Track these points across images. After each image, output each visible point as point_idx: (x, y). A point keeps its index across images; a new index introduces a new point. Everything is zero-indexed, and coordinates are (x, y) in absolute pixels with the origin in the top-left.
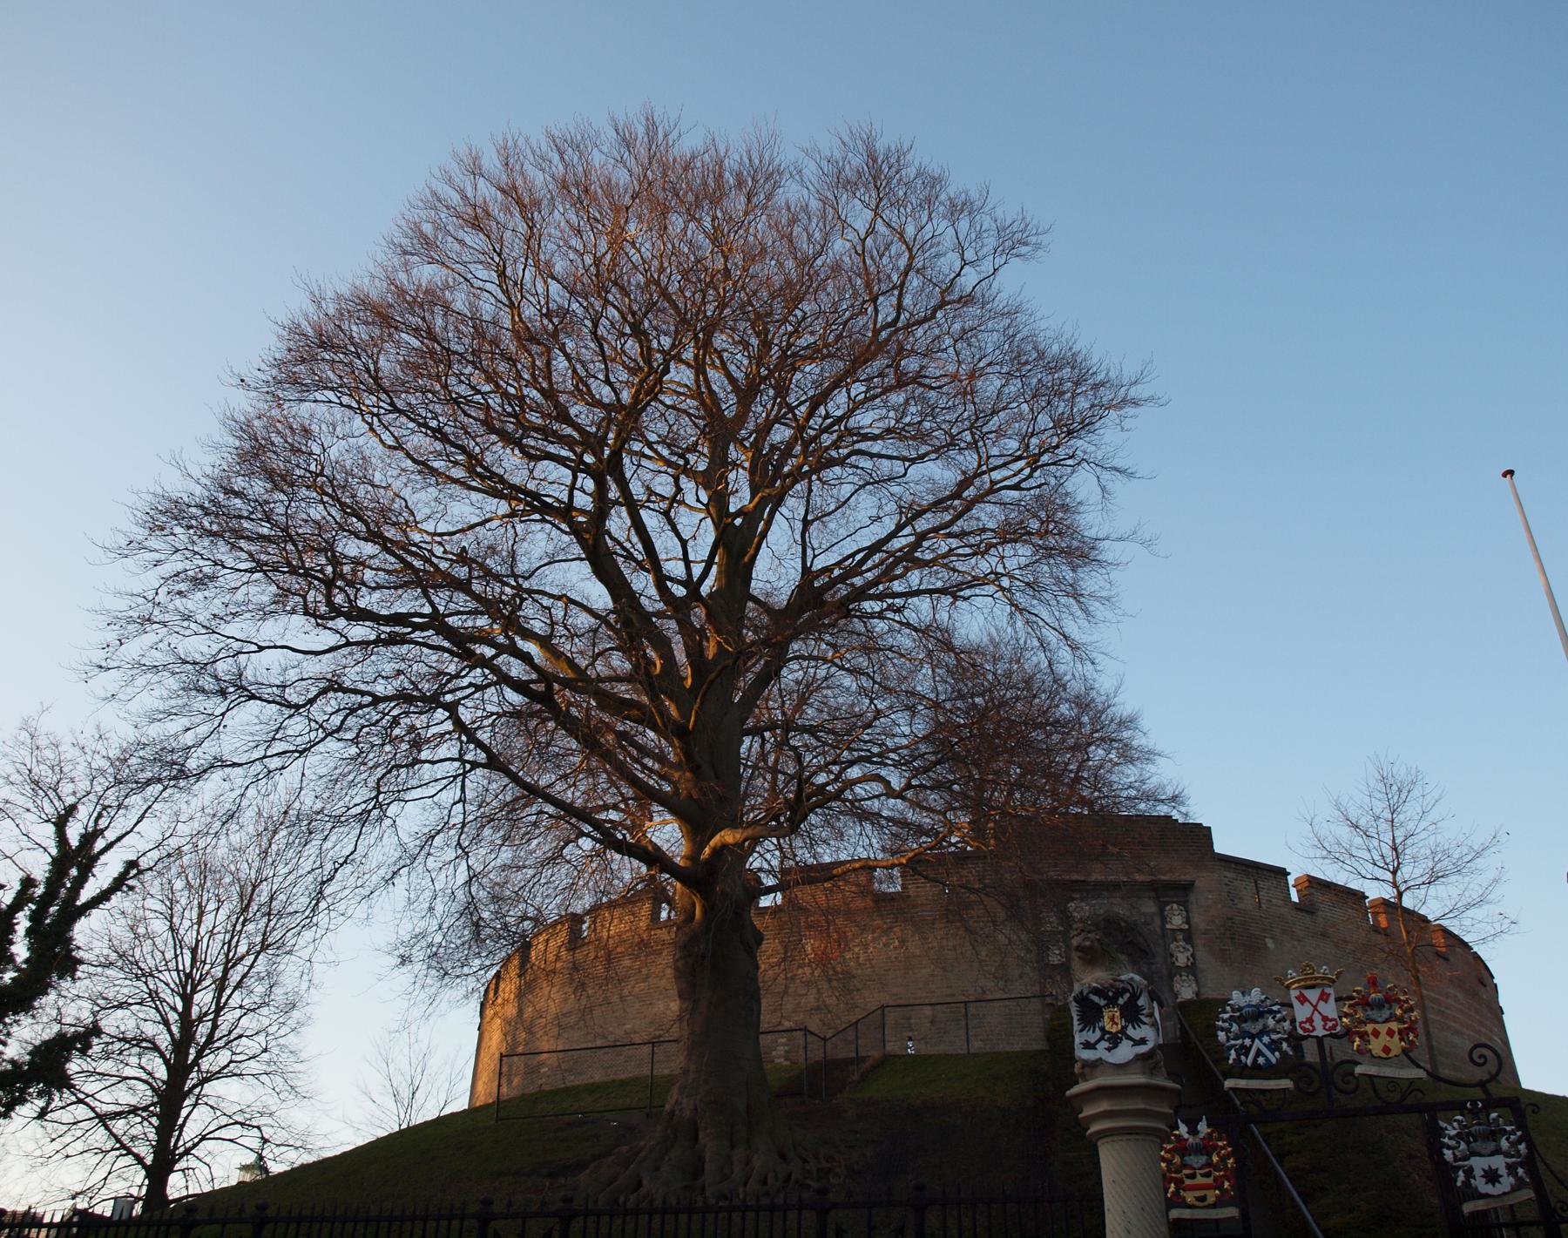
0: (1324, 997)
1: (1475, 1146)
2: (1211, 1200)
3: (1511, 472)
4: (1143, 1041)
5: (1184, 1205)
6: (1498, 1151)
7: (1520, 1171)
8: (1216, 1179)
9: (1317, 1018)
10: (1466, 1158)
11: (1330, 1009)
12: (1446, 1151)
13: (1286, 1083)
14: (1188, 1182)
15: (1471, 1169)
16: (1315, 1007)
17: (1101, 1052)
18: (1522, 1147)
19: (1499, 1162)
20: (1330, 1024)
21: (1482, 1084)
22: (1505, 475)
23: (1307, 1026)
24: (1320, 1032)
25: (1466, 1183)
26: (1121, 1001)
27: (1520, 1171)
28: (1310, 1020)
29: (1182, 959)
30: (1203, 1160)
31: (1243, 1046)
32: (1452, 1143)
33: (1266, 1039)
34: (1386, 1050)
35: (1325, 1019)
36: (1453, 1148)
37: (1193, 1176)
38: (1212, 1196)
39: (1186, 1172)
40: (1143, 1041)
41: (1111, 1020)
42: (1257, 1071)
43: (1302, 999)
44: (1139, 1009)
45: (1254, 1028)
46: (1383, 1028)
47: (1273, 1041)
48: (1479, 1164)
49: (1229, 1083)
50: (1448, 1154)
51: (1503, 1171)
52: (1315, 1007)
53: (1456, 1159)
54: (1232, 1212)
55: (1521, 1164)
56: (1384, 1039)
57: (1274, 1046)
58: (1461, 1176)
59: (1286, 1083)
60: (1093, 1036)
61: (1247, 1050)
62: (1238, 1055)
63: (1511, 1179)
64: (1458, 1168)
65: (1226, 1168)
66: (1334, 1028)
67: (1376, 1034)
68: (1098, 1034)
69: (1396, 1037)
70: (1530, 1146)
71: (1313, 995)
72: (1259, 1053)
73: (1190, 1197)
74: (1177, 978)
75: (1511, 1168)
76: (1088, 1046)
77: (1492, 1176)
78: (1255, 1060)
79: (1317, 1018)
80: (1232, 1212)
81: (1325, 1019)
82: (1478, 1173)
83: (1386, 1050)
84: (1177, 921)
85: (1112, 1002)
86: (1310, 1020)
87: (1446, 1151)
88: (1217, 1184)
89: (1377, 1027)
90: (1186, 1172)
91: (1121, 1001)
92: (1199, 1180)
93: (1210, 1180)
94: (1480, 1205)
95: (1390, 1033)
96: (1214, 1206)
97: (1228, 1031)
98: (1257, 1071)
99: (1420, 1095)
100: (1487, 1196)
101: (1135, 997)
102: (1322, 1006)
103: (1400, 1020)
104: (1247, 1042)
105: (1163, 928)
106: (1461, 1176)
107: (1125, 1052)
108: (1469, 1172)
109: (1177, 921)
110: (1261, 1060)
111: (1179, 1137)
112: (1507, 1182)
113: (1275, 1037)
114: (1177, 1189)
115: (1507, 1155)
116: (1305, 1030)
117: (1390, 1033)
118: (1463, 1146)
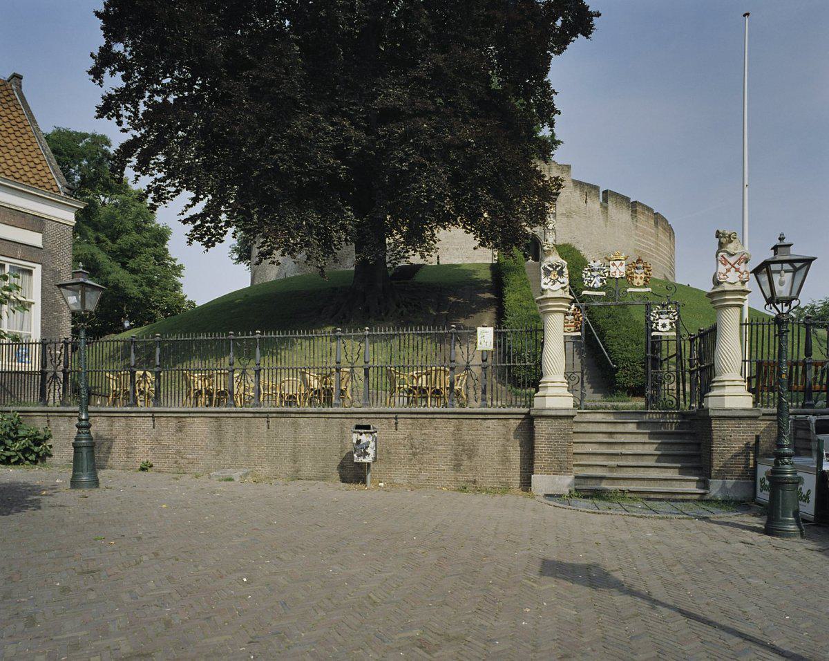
0: (621, 264)
1: (661, 316)
3: (748, 14)
4: (563, 283)
9: (618, 271)
11: (623, 269)
13: (603, 293)
15: (658, 323)
17: (549, 286)
18: (676, 318)
22: (744, 16)
24: (618, 277)
25: (656, 327)
26: (557, 269)
28: (615, 272)
33: (599, 278)
35: (620, 272)
40: (563, 283)
41: (554, 276)
42: (592, 289)
44: (563, 272)
46: (639, 276)
48: (661, 322)
49: (584, 292)
50: (652, 318)
51: (668, 324)
53: (654, 320)
54: (579, 334)
57: (602, 281)
58: (654, 325)
59: (603, 293)
60: (546, 280)
61: (591, 281)
63: (670, 327)
67: (636, 278)
70: (679, 317)
71: (617, 263)
75: (671, 324)
76: (545, 284)
77: (664, 326)
79: (618, 271)
81: (620, 272)
83: (638, 283)
85: (555, 269)
86: (615, 272)
91: (557, 269)
92: (569, 324)
97: (586, 274)
98: (592, 289)
100: (661, 331)
101: (562, 268)
104: (592, 279)
106: (654, 325)
107: (558, 286)
108: (657, 324)
110: (595, 286)
112: (668, 327)
115: (671, 319)
117: (641, 278)
118: (657, 316)
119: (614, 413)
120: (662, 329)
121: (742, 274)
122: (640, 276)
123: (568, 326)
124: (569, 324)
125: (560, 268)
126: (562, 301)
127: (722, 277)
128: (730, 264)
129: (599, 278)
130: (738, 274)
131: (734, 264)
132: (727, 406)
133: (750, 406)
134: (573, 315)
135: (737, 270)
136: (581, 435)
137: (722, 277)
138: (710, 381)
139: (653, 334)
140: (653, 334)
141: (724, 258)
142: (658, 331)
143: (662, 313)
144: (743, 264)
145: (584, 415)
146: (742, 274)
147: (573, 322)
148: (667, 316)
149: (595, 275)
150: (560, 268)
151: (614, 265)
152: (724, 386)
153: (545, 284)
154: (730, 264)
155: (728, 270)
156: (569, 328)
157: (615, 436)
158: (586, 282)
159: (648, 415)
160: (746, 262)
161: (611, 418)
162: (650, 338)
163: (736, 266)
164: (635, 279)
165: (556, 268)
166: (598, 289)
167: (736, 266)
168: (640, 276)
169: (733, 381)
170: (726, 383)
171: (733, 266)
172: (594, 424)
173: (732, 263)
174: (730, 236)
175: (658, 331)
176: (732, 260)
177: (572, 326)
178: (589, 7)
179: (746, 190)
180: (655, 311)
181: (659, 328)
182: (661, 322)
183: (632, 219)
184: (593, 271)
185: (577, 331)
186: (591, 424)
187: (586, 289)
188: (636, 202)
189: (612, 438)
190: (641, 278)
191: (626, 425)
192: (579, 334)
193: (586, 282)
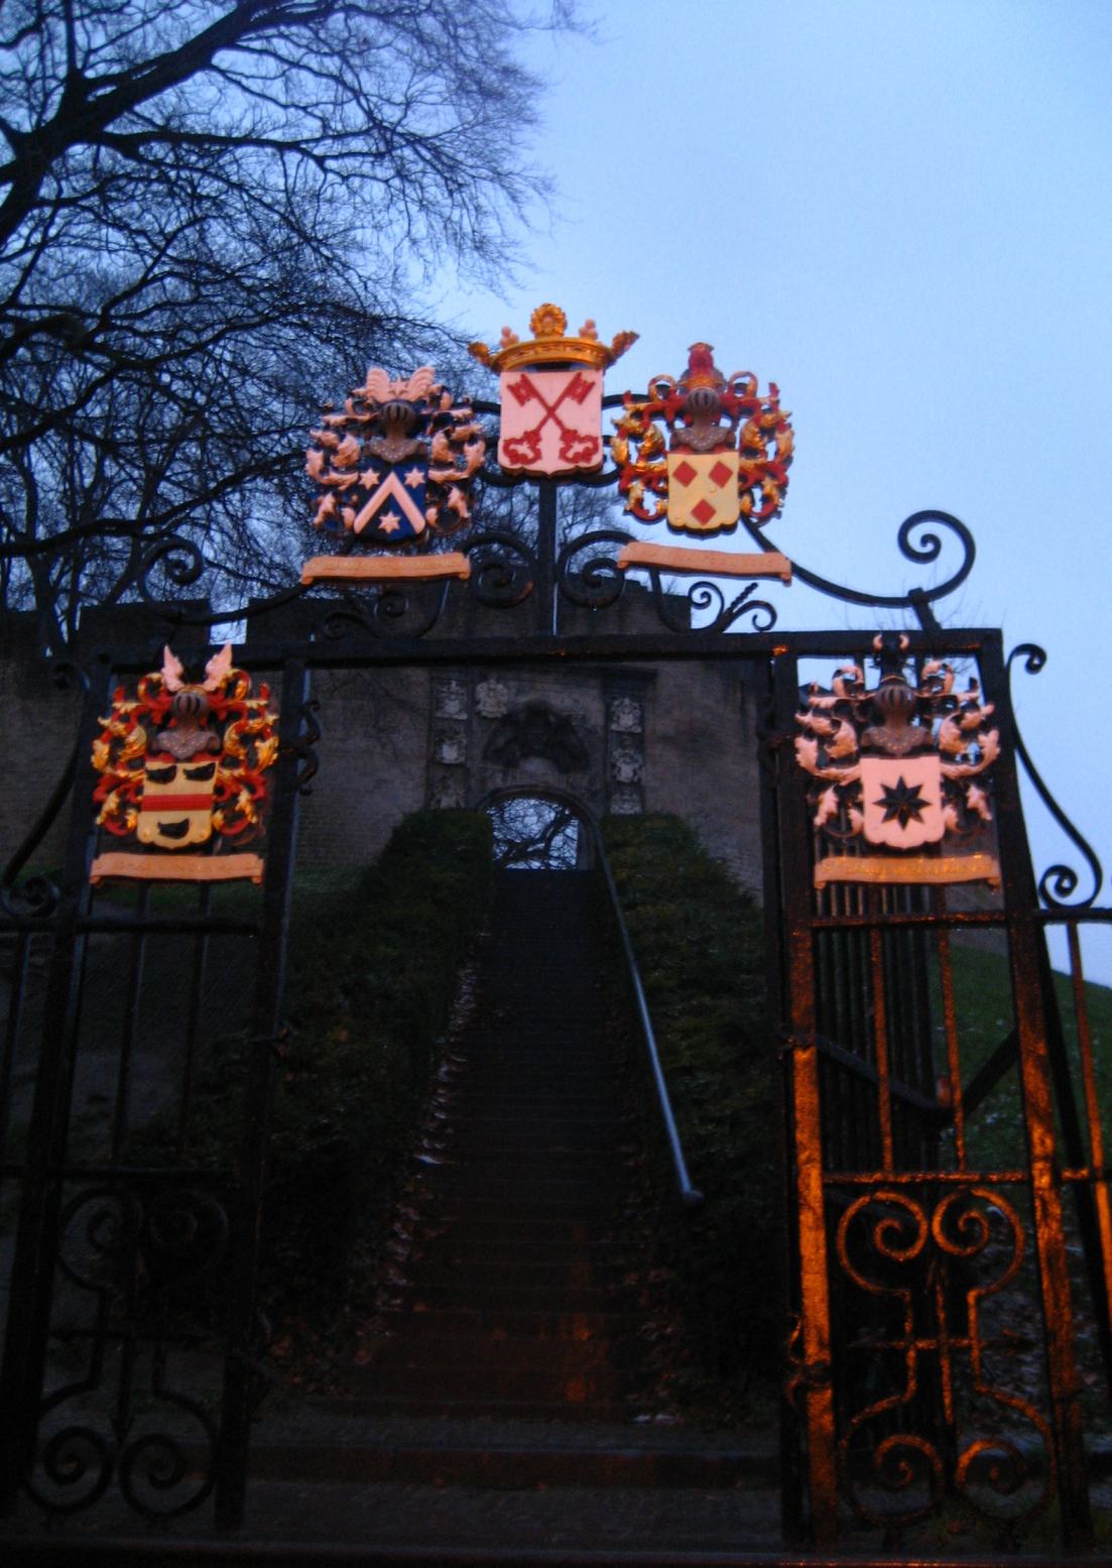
0: (578, 391)
5: (130, 843)
7: (975, 796)
8: (219, 789)
10: (850, 760)
14: (151, 789)
15: (857, 785)
16: (551, 412)
19: (926, 773)
20: (578, 447)
21: (919, 600)
24: (550, 461)
25: (838, 819)
27: (975, 796)
28: (533, 437)
29: (626, 772)
30: (201, 739)
31: (356, 487)
32: (822, 724)
33: (415, 477)
34: (704, 510)
35: (569, 436)
36: (824, 739)
37: (165, 777)
38: (201, 826)
39: (154, 765)
43: (524, 392)
45: (393, 449)
46: (703, 463)
47: (430, 485)
48: (875, 775)
50: (807, 751)
51: (932, 793)
52: (551, 412)
53: (825, 761)
54: (249, 865)
55: (978, 779)
56: (702, 488)
58: (829, 801)
61: (366, 494)
63: (950, 814)
64: (823, 784)
65: (252, 760)
66: (587, 455)
67: (686, 475)
69: (733, 484)
71: (551, 385)
72: (391, 504)
73: (146, 825)
74: (616, 796)
75: (954, 790)
77: (903, 803)
80: (249, 865)
81: (569, 436)
82: (872, 793)
83: (704, 510)
84: (627, 721)
86: (533, 437)
88: (223, 798)
89: (694, 460)
90: (154, 765)
92: (181, 785)
93: (207, 787)
94: (864, 869)
95: (720, 475)
96: (204, 849)
99: (764, 618)
100: (884, 850)
102: (570, 413)
103: (749, 450)
105: (606, 727)
106: (829, 801)
108: (850, 793)
109: (627, 721)
110: (390, 522)
111: (156, 688)
112: (935, 821)
113: (436, 475)
114: (124, 806)
115: (947, 756)
116: (515, 457)
118: (846, 731)
129: (415, 477)
139: (831, 869)
140: (831, 869)
149: (392, 456)
156: (172, 817)
164: (674, 486)
166: (406, 541)
181: (875, 825)
185: (231, 849)
190: (720, 475)
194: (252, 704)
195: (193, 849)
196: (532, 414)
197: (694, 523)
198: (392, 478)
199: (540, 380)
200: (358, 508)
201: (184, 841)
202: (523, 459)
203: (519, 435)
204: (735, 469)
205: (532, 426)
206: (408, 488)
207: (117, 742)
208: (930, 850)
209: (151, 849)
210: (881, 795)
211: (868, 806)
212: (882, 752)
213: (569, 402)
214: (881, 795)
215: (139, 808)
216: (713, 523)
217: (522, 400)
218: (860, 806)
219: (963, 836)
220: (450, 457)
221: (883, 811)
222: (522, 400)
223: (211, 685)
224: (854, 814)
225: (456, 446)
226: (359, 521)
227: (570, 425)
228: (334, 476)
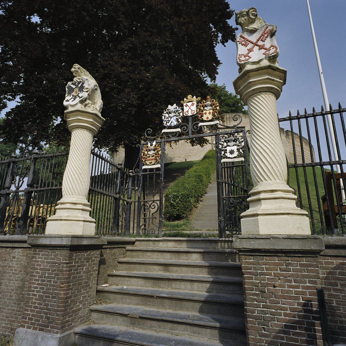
0: (193, 105)
1: (229, 144)
2: (153, 163)
5: (146, 165)
6: (236, 145)
7: (241, 150)
9: (190, 111)
10: (226, 147)
11: (194, 108)
12: (220, 145)
13: (179, 130)
14: (148, 158)
15: (226, 150)
18: (243, 144)
19: (235, 148)
20: (193, 112)
23: (187, 113)
25: (224, 154)
26: (79, 86)
27: (241, 150)
28: (188, 111)
32: (222, 143)
33: (175, 118)
34: (207, 118)
35: (192, 111)
37: (149, 157)
38: (153, 162)
42: (170, 127)
46: (208, 112)
48: (229, 149)
49: (164, 131)
51: (236, 151)
56: (208, 115)
58: (223, 152)
59: (179, 130)
61: (169, 121)
62: (166, 123)
64: (223, 150)
66: (194, 112)
67: (206, 113)
68: (72, 96)
69: (211, 114)
71: (189, 104)
72: (172, 122)
73: (148, 162)
75: (238, 150)
77: (232, 152)
78: (171, 124)
79: (190, 111)
81: (192, 111)
82: (228, 151)
83: (207, 118)
86: (188, 111)
87: (220, 145)
90: (148, 156)
91: (79, 86)
92: (151, 158)
93: (154, 158)
98: (170, 127)
100: (229, 158)
104: (169, 119)
106: (223, 152)
110: (172, 124)
112: (236, 154)
113: (177, 117)
115: (238, 146)
119: (187, 241)
120: (231, 156)
121: (269, 50)
122: (209, 111)
123: (149, 160)
124: (151, 158)
125: (81, 83)
126: (81, 116)
127: (243, 58)
128: (252, 43)
129: (175, 118)
130: (263, 51)
131: (258, 40)
132: (263, 231)
133: (307, 232)
134: (154, 150)
135: (261, 48)
136: (138, 266)
137: (243, 58)
138: (246, 193)
139: (223, 160)
140: (223, 160)
141: (244, 38)
142: (227, 158)
143: (229, 141)
144: (268, 39)
145: (156, 243)
146: (269, 50)
147: (153, 156)
148: (234, 143)
150: (81, 83)
151: (187, 106)
152: (259, 200)
153: (68, 101)
154: (252, 43)
155: (250, 50)
157: (171, 268)
158: (165, 123)
159: (219, 244)
160: (271, 36)
161: (184, 247)
162: (220, 165)
163: (260, 43)
165: (78, 85)
167: (260, 43)
168: (209, 111)
169: (273, 191)
170: (262, 196)
171: (256, 44)
172: (159, 254)
173: (254, 41)
174: (248, 12)
175: (227, 158)
176: (254, 38)
177: (152, 160)
178: (232, 26)
179: (322, 76)
180: (223, 140)
181: (228, 155)
182: (229, 149)
183: (286, 138)
184: (170, 113)
186: (156, 253)
187: (164, 127)
188: (288, 130)
189: (168, 271)
190: (210, 113)
191: (189, 255)
192: (159, 166)
193: (165, 123)
194: (158, 147)
195: (153, 165)
196: (188, 108)
197: (206, 120)
198: (172, 119)
199: (188, 104)
200: (168, 123)
201: (152, 164)
202: (187, 114)
203: (186, 111)
204: (212, 112)
205: (187, 110)
206: (174, 119)
207: (144, 153)
208: (235, 157)
209: (148, 165)
210: (229, 151)
211: (228, 153)
212: (230, 146)
213: (192, 106)
214: (229, 151)
215: (147, 160)
216: (209, 119)
217: (186, 107)
218: (227, 153)
219: (240, 156)
220: (179, 115)
221: (234, 153)
222: (186, 107)
223: (153, 146)
224: (226, 154)
225: (179, 113)
226: (169, 124)
227: (192, 109)
228: (166, 119)
